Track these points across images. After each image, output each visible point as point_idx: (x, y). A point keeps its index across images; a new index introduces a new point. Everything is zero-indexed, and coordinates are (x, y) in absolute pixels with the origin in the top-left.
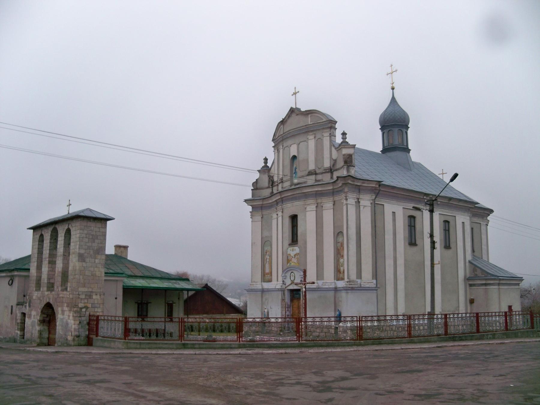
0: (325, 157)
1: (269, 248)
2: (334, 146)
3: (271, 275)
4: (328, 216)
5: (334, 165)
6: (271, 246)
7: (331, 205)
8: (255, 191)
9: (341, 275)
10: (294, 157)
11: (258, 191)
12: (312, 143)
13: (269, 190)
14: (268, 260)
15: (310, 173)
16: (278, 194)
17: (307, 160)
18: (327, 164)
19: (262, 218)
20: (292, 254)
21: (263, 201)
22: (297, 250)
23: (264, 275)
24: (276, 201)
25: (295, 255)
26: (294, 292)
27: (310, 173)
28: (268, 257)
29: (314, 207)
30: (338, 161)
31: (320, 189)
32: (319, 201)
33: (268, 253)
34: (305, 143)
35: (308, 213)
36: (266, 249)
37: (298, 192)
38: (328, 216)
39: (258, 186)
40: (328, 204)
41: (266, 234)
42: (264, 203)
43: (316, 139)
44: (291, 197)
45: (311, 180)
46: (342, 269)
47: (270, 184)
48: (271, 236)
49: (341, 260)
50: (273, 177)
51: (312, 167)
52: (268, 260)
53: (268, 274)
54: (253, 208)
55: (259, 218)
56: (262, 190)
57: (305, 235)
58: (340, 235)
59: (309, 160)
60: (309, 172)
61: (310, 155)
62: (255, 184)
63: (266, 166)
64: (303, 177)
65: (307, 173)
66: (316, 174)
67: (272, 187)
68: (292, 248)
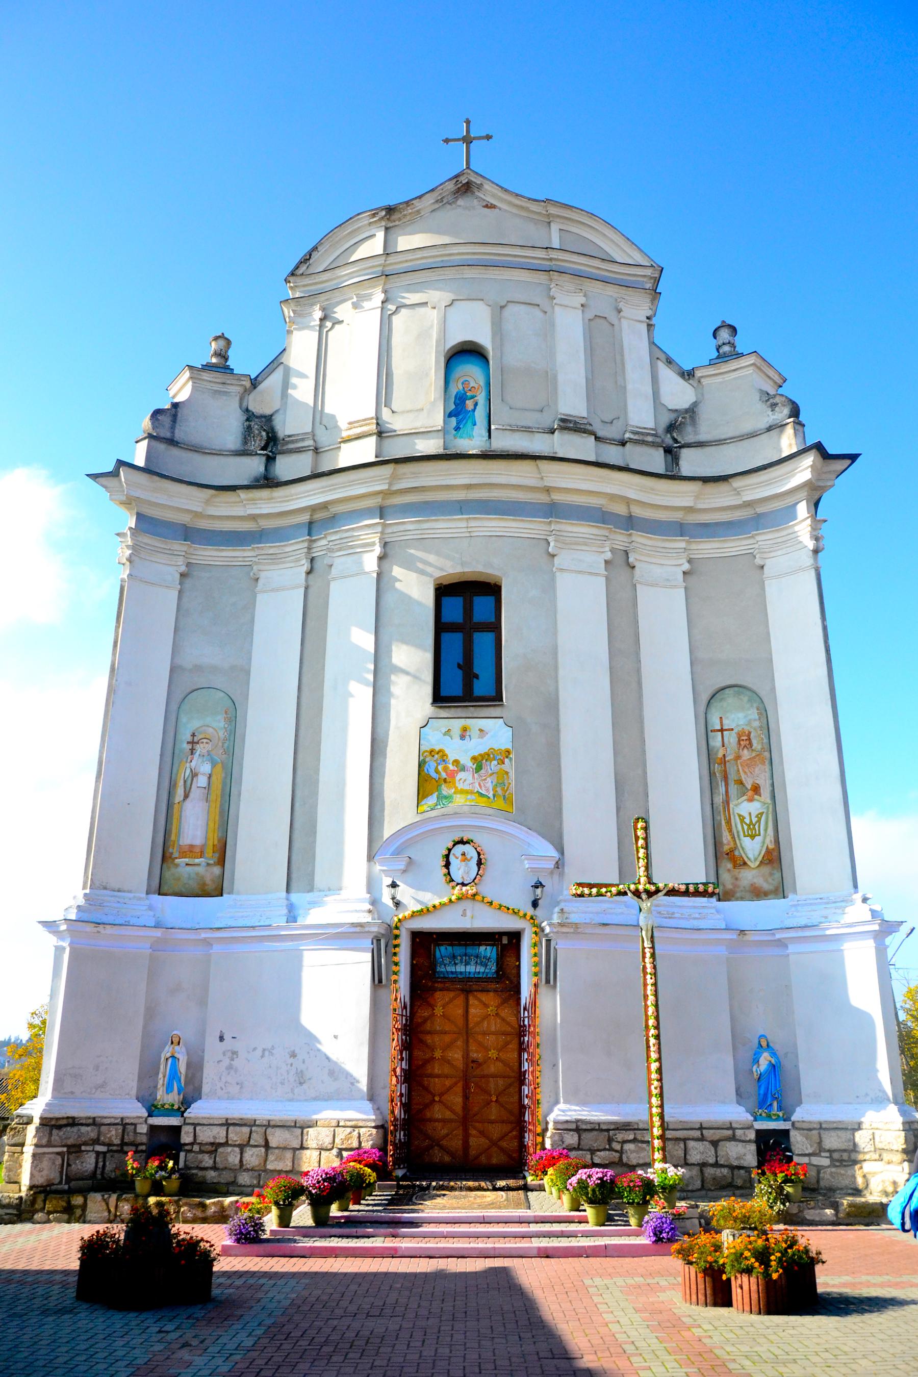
0: (630, 387)
1: (216, 724)
2: (669, 361)
3: (222, 862)
4: (664, 612)
5: (671, 428)
6: (234, 715)
7: (675, 567)
8: (162, 447)
9: (748, 877)
10: (468, 352)
11: (175, 451)
12: (569, 324)
13: (255, 466)
14: (202, 781)
15: (570, 425)
16: (387, 470)
17: (549, 379)
18: (642, 415)
19: (183, 575)
20: (460, 751)
21: (208, 502)
22: (491, 731)
23: (166, 858)
24: (314, 509)
25: (480, 762)
26: (443, 951)
27: (570, 425)
28: (206, 768)
29: (596, 559)
30: (705, 415)
31: (632, 495)
32: (620, 539)
33: (199, 749)
34: (537, 312)
35: (564, 582)
36: (189, 725)
37: (514, 481)
38: (664, 612)
39: (179, 435)
40: (661, 566)
41: (203, 652)
42: (212, 511)
43: (590, 315)
44: (461, 495)
45: (584, 447)
46: (752, 848)
47: (255, 445)
48: (243, 673)
49: (746, 809)
50: (269, 419)
51: (573, 404)
52: (202, 781)
53: (190, 851)
54: (140, 517)
55: (171, 570)
56: (197, 458)
57: (548, 668)
58: (730, 699)
59: (561, 378)
60: (563, 420)
61: (560, 358)
62: (166, 420)
63: (221, 366)
64: (528, 430)
65: (548, 419)
66: (597, 438)
67: (270, 460)
68: (456, 725)
